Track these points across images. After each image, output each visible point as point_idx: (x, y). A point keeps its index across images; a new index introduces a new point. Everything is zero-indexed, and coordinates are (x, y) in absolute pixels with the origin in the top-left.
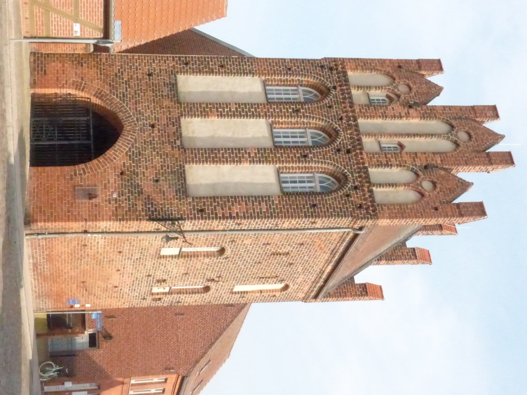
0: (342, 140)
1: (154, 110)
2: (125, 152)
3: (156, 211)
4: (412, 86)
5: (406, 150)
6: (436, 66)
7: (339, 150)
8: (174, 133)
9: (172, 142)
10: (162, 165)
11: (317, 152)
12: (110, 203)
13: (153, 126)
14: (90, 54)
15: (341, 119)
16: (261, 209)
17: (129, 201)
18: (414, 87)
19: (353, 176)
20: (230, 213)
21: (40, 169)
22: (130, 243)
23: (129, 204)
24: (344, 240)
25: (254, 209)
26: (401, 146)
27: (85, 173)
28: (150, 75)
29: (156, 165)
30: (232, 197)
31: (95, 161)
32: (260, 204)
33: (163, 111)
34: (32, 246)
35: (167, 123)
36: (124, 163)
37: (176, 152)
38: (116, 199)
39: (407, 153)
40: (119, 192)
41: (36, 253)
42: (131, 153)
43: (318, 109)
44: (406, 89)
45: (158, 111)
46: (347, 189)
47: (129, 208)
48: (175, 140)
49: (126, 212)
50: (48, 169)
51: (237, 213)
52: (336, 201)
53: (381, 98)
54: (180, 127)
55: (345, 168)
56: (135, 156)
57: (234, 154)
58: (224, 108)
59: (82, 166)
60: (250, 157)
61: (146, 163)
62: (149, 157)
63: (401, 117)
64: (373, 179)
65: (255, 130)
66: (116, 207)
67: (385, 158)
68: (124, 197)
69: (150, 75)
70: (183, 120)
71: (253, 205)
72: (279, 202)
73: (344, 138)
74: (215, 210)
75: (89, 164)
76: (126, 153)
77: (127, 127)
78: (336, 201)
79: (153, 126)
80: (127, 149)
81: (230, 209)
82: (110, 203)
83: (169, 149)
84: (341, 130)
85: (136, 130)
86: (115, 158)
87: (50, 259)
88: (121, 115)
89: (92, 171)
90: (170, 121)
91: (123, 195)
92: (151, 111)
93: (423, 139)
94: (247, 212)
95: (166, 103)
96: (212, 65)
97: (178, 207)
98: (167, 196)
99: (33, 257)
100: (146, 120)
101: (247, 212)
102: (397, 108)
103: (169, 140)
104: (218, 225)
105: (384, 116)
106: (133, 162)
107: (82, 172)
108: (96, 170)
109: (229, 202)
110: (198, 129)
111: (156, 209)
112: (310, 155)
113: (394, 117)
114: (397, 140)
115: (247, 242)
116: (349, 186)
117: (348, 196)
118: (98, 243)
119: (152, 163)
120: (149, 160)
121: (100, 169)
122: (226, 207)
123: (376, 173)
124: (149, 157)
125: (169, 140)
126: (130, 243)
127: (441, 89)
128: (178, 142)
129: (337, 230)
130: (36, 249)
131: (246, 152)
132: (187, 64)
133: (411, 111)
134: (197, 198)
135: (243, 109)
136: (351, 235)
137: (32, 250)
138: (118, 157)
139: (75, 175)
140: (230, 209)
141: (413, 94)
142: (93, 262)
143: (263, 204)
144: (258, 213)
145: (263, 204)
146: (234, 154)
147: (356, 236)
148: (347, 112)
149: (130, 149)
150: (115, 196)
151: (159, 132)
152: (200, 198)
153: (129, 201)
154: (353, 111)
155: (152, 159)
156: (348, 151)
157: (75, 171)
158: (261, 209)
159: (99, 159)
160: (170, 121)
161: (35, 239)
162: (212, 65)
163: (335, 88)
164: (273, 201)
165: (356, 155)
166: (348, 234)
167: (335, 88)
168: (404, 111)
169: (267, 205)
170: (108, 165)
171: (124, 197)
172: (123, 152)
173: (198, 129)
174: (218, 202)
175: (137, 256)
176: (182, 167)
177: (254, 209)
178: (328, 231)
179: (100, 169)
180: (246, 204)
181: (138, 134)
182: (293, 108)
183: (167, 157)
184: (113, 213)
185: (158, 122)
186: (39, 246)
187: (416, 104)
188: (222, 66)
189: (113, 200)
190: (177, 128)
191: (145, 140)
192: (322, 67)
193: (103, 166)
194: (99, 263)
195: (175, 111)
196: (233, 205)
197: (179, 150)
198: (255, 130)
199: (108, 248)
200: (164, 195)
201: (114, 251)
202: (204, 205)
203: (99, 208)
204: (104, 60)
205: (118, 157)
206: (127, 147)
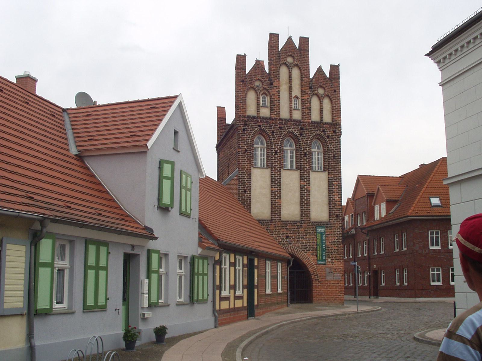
0: (295, 131)
1: (277, 235)
2: (304, 253)
3: (338, 240)
8: (292, 225)
9: (298, 227)
10: (312, 234)
11: (303, 147)
12: (334, 263)
13: (287, 237)
15: (280, 128)
16: (337, 185)
17: (333, 253)
19: (317, 131)
20: (339, 201)
23: (334, 253)
29: (312, 237)
31: (310, 269)
33: (278, 230)
35: (285, 228)
36: (311, 254)
38: (331, 259)
40: (328, 258)
42: (305, 250)
43: (275, 140)
45: (278, 233)
46: (325, 136)
47: (336, 253)
48: (296, 225)
50: (314, 295)
52: (331, 144)
54: (288, 221)
55: (312, 134)
56: (306, 248)
60: (306, 185)
61: (310, 242)
62: (307, 241)
65: (290, 180)
66: (336, 260)
67: (306, 109)
68: (331, 255)
71: (334, 189)
72: (333, 174)
73: (295, 130)
74: (337, 209)
75: (312, 273)
76: (305, 252)
78: (331, 144)
80: (303, 252)
82: (334, 263)
84: (289, 130)
85: (291, 247)
86: (308, 259)
89: (316, 271)
90: (284, 227)
91: (329, 256)
92: (278, 237)
96: (245, 197)
97: (335, 228)
98: (329, 233)
100: (284, 240)
102: (273, 92)
103: (297, 229)
106: (311, 249)
107: (316, 277)
111: (336, 240)
112: (305, 151)
116: (323, 134)
119: (311, 239)
120: (309, 241)
121: (314, 267)
122: (335, 203)
124: (307, 241)
125: (297, 229)
128: (298, 224)
135: (276, 184)
138: (307, 257)
139: (318, 280)
140: (337, 201)
141: (263, 79)
144: (338, 187)
149: (303, 250)
150: (329, 260)
151: (292, 234)
153: (333, 253)
154: (276, 119)
155: (308, 239)
156: (302, 129)
157: (316, 280)
158: (337, 185)
159: (308, 267)
160: (284, 227)
162: (245, 197)
163: (259, 126)
165: (304, 125)
169: (334, 182)
170: (312, 262)
171: (331, 255)
172: (304, 254)
176: (314, 223)
179: (314, 267)
180: (334, 192)
181: (293, 245)
182: (275, 154)
183: (307, 231)
185: (285, 233)
188: (245, 191)
189: (332, 261)
190: (289, 223)
191: (297, 242)
193: (313, 265)
195: (278, 223)
196: (335, 199)
197: (303, 224)
200: (329, 235)
202: (335, 214)
203: (336, 268)
205: (307, 257)
206: (301, 252)
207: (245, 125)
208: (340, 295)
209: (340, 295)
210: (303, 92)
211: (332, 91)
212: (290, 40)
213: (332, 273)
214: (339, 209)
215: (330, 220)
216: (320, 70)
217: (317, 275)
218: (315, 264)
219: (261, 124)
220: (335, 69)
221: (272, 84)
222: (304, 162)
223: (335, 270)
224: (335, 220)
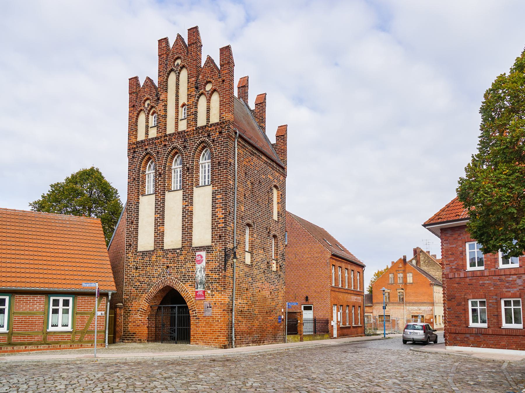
4: (145, 98)
5: (186, 103)
6: (134, 81)
7: (185, 147)
14: (124, 305)
15: (165, 145)
16: (220, 198)
18: (147, 96)
19: (201, 138)
20: (222, 218)
21: (192, 338)
22: (241, 283)
24: (244, 146)
25: (220, 203)
26: (184, 105)
27: (195, 310)
28: (137, 268)
30: (212, 217)
31: (188, 304)
32: (218, 199)
34: (241, 344)
37: (184, 252)
39: (188, 101)
41: (245, 341)
44: (148, 102)
49: (219, 285)
50: (192, 333)
51: (222, 214)
53: (153, 119)
54: (169, 250)
57: (187, 215)
58: (158, 222)
59: (191, 312)
60: (188, 205)
63: (166, 106)
64: (205, 124)
69: (137, 268)
70: (165, 248)
71: (218, 203)
73: (178, 144)
76: (184, 284)
77: (168, 283)
79: (168, 267)
81: (220, 219)
83: (182, 258)
87: (250, 334)
88: (161, 287)
93: (181, 91)
94: (221, 207)
95: (154, 258)
99: (248, 343)
101: (221, 207)
102: (160, 107)
104: (230, 227)
105: (165, 116)
108: (193, 303)
109: (215, 219)
110: (173, 239)
113: (165, 110)
114: (180, 109)
115: (243, 209)
117: (214, 141)
118: (240, 303)
123: (201, 121)
126: (241, 283)
127: (148, 78)
128: (178, 251)
129: (236, 149)
130: (242, 342)
131: (184, 208)
132: (131, 245)
133: (161, 98)
134: (212, 240)
136: (239, 140)
137: (243, 344)
139: (196, 316)
140: (220, 219)
142: (253, 307)
143: (217, 197)
145: (217, 197)
146: (187, 215)
147: (240, 136)
148: (161, 142)
150: (209, 292)
152: (212, 237)
154: (161, 137)
157: (193, 316)
158: (220, 198)
161: (235, 342)
163: (146, 149)
164: (216, 191)
166: (240, 142)
167: (146, 149)
168: (161, 103)
173: (173, 239)
174: (215, 226)
175: (250, 279)
177: (220, 203)
178: (236, 155)
180: (217, 208)
184: (220, 293)
186: (240, 339)
187: (157, 96)
192: (133, 157)
193: (191, 299)
194: (254, 303)
196: (217, 216)
198: (174, 201)
199: (244, 297)
201: (246, 293)
202: (217, 235)
204: (128, 297)
207: (134, 152)
208: (219, 336)
209: (219, 336)
210: (189, 96)
211: (219, 82)
212: (179, 38)
213: (210, 307)
214: (222, 227)
215: (212, 242)
216: (210, 60)
217: (195, 310)
218: (193, 298)
219: (147, 147)
220: (226, 52)
221: (159, 99)
222: (189, 178)
223: (215, 304)
224: (217, 242)
